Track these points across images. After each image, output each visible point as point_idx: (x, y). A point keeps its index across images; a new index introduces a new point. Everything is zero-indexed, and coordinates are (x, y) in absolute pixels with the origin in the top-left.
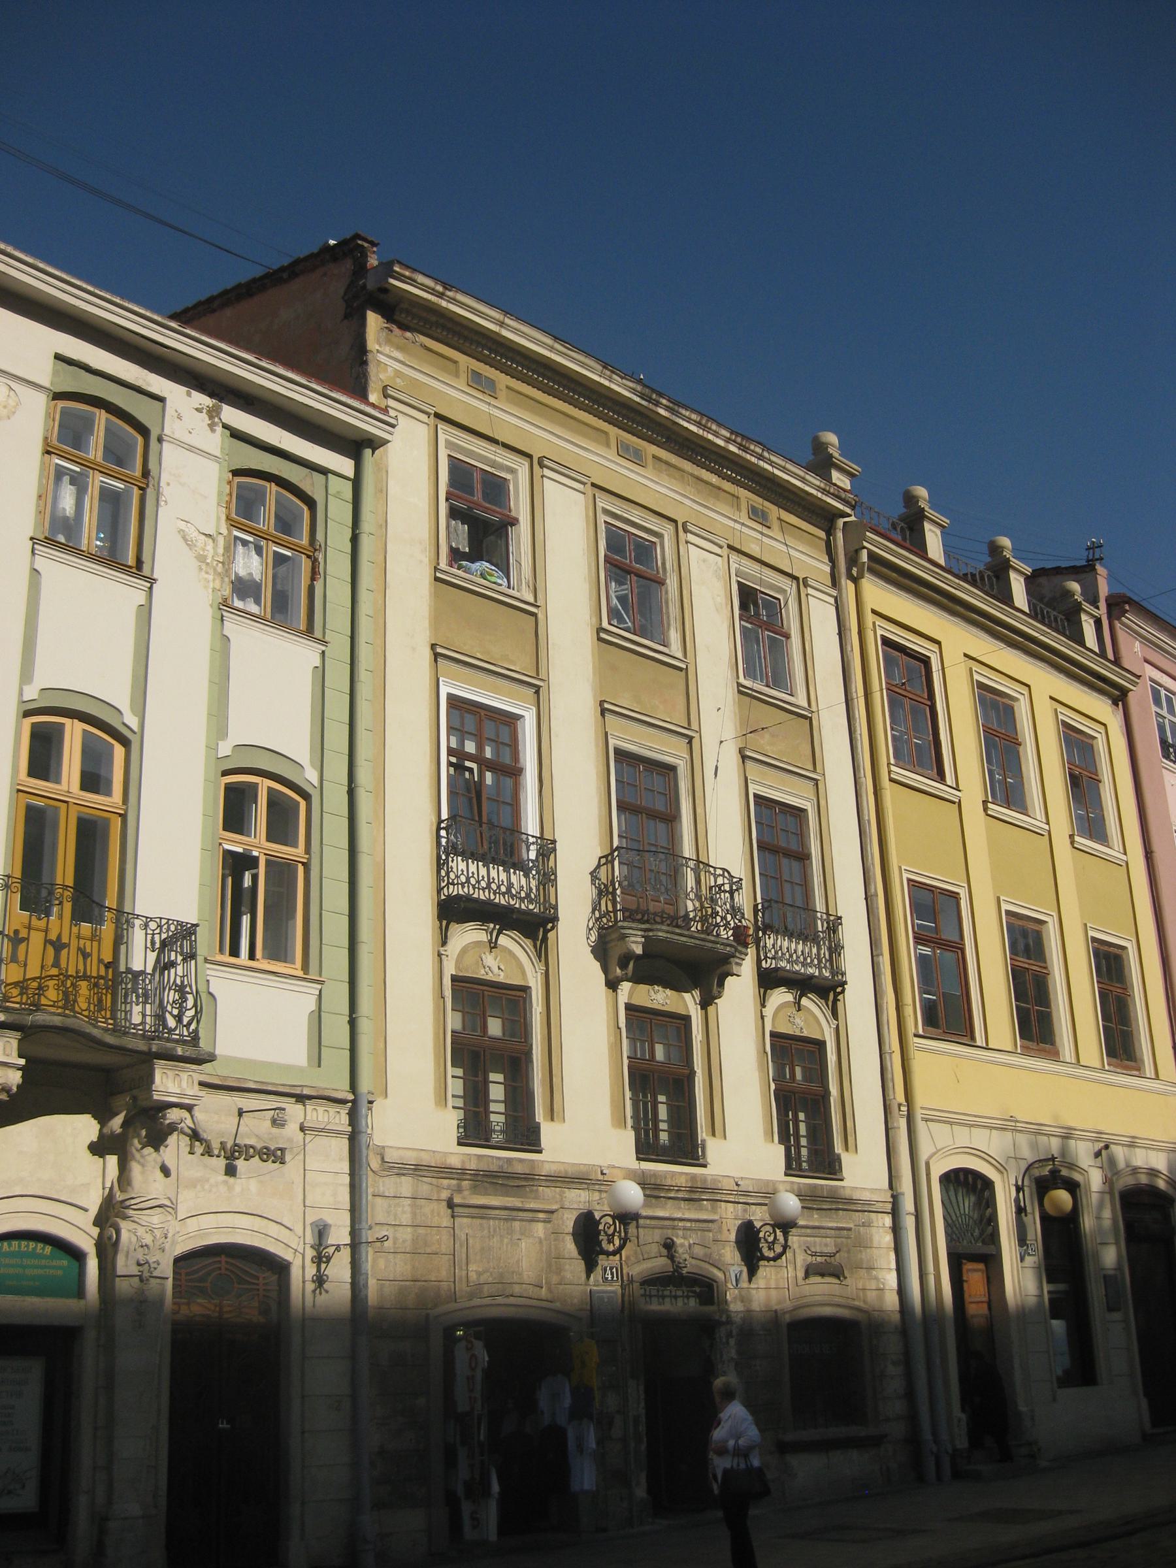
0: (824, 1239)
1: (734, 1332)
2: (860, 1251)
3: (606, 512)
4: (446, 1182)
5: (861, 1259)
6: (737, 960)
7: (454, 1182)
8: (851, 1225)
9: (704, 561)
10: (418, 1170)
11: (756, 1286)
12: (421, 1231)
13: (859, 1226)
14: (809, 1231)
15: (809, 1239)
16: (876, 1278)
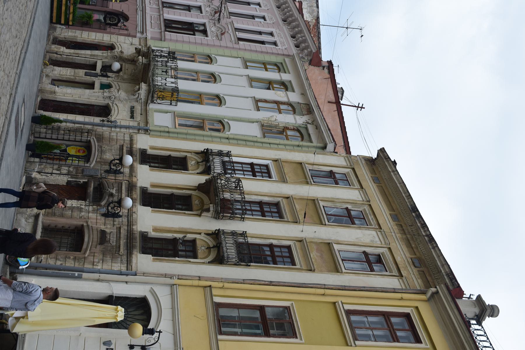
0: (115, 241)
1: (82, 206)
2: (110, 257)
3: (365, 210)
4: (129, 145)
5: (107, 257)
6: (215, 207)
7: (129, 147)
8: (121, 252)
9: (374, 237)
10: (131, 140)
11: (98, 215)
12: (116, 140)
13: (121, 258)
14: (118, 235)
15: (115, 235)
16: (98, 262)
